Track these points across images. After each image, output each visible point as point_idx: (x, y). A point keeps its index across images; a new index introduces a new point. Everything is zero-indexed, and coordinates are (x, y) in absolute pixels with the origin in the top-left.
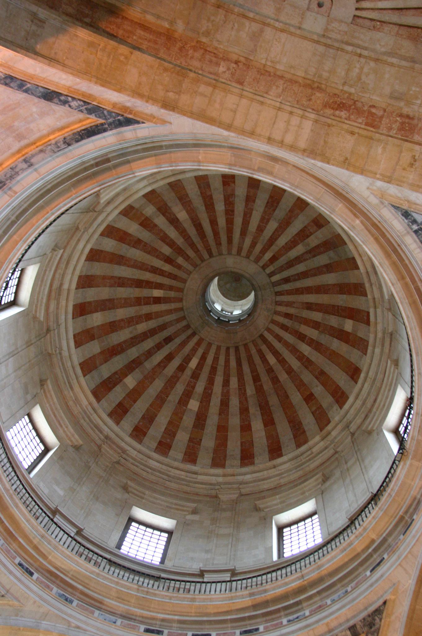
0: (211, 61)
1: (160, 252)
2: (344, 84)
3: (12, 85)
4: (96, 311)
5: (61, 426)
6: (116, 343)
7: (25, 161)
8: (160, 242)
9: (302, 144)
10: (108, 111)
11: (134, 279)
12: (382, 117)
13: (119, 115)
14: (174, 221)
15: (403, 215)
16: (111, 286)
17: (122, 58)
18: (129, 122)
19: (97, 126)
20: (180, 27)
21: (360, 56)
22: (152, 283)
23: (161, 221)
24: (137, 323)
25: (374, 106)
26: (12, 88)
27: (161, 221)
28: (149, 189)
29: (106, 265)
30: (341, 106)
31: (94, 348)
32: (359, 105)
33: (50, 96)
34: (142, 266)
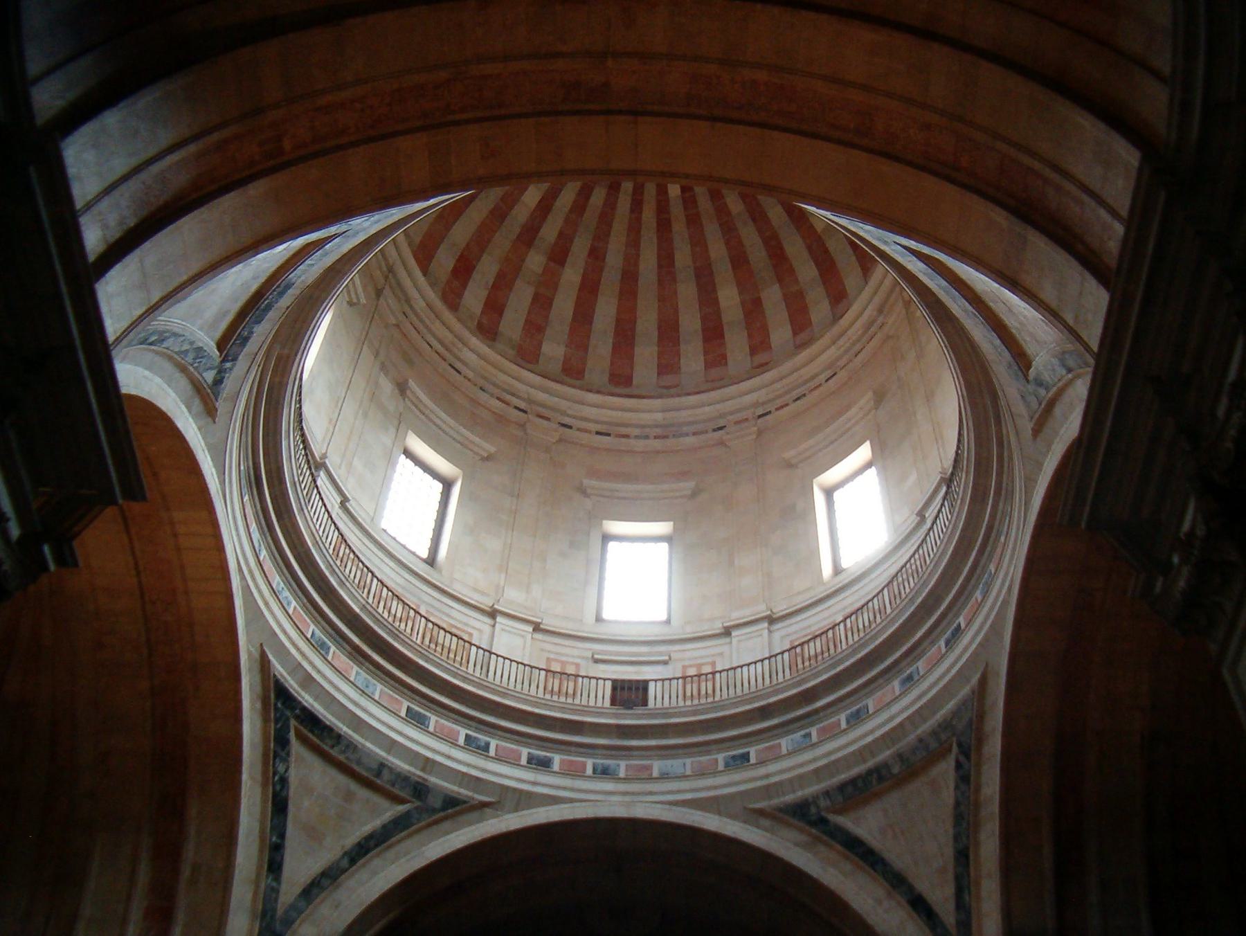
1: (605, 204)
4: (716, 302)
5: (849, 429)
6: (764, 253)
7: (379, 774)
8: (587, 214)
10: (276, 723)
11: (659, 238)
13: (276, 709)
14: (545, 207)
16: (674, 280)
18: (282, 693)
19: (301, 722)
22: (659, 202)
23: (549, 232)
24: (729, 213)
27: (549, 232)
28: (474, 341)
29: (641, 303)
31: (772, 296)
33: (279, 806)
34: (635, 228)
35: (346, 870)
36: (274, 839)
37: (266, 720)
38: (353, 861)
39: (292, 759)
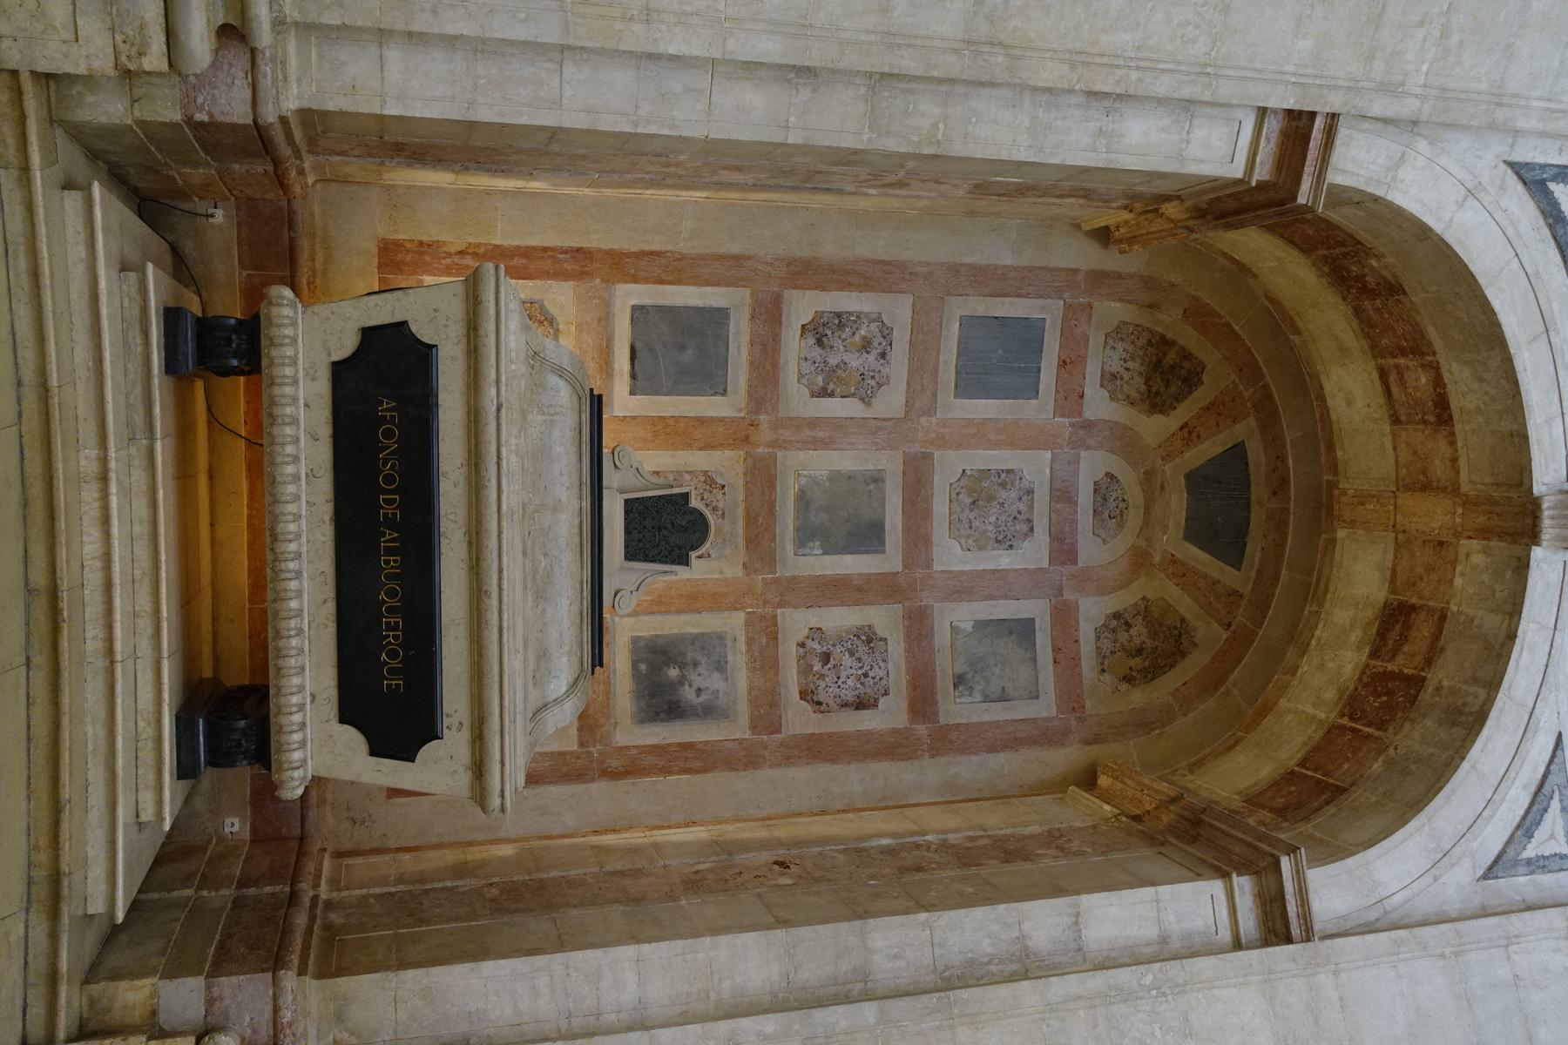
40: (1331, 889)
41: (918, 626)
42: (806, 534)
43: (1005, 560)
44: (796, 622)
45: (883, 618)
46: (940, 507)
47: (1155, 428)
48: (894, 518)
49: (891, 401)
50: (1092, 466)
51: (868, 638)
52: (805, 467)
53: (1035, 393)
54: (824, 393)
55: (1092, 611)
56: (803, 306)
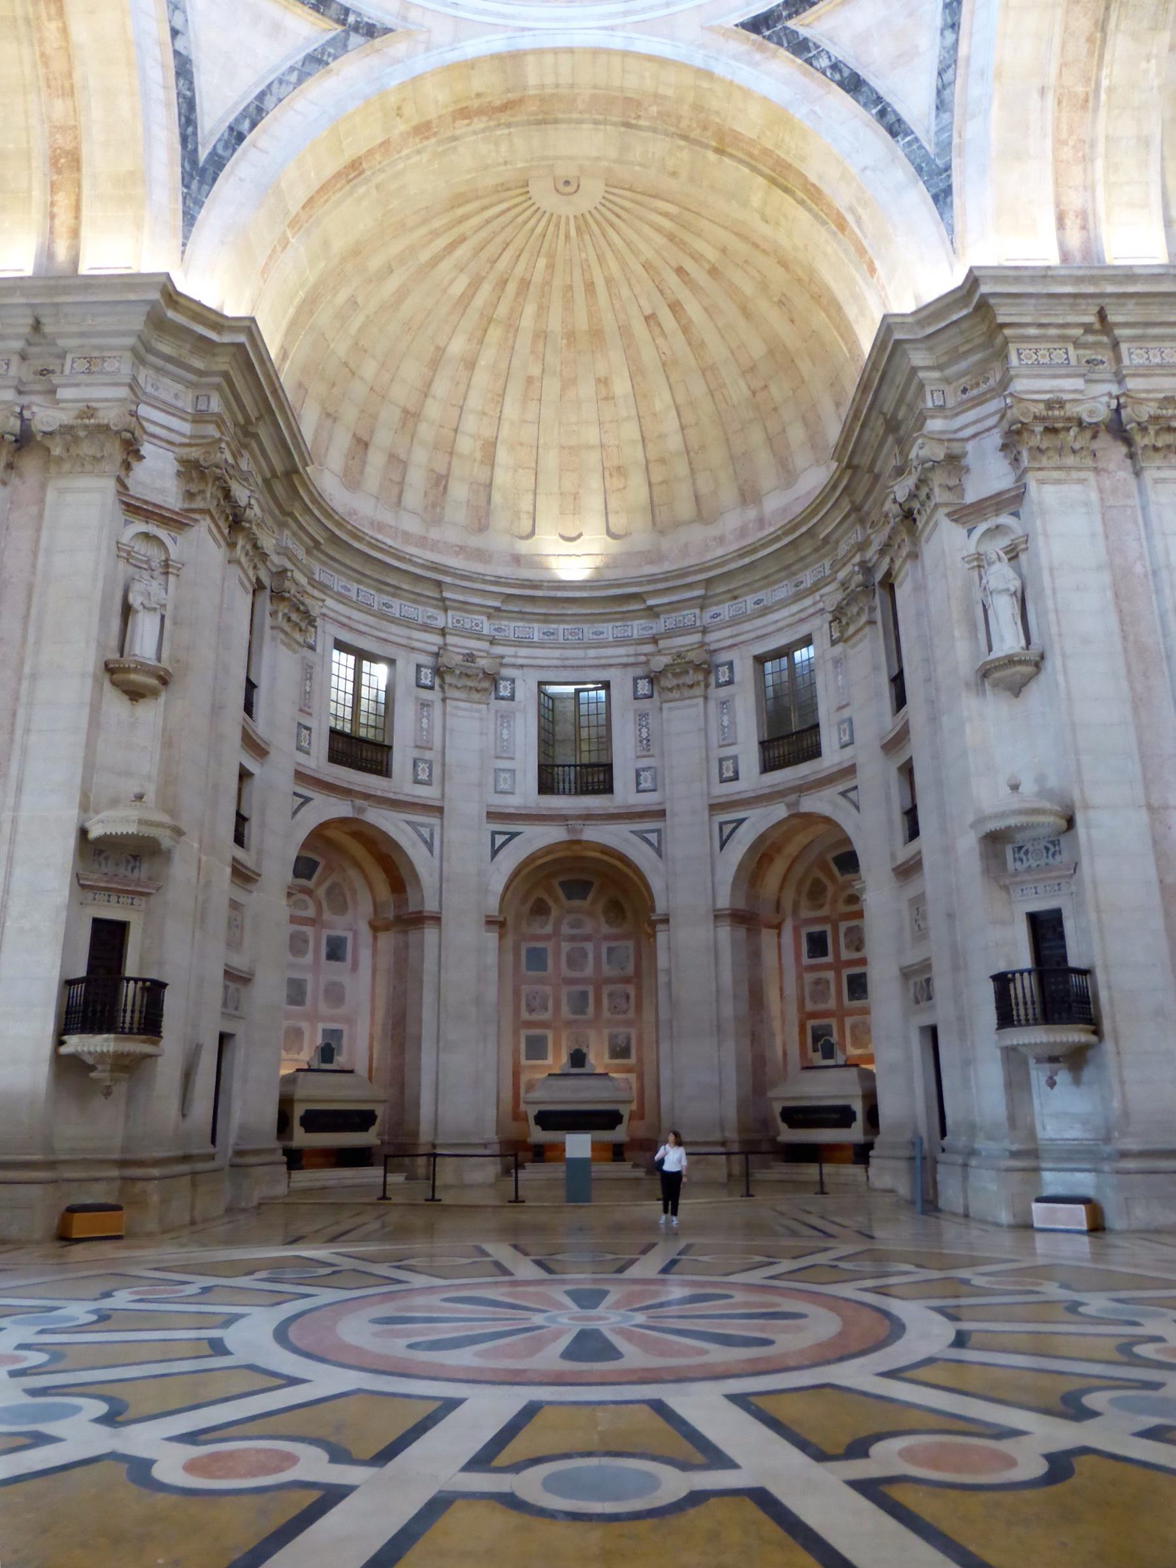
0: (669, 116)
2: (510, 134)
3: (891, 118)
9: (531, 60)
12: (454, 121)
13: (769, 38)
15: (374, 25)
17: (768, 133)
18: (757, 25)
19: (797, 13)
20: (712, 156)
21: (506, 163)
25: (468, 125)
26: (894, 112)
30: (505, 107)
32: (484, 118)
33: (853, 84)
35: (957, 40)
36: (874, 111)
37: (775, 55)
38: (954, 26)
39: (825, 44)
40: (661, 906)
41: (609, 981)
42: (583, 1012)
43: (591, 956)
44: (606, 1014)
45: (606, 990)
46: (576, 974)
47: (555, 912)
48: (579, 988)
49: (548, 989)
50: (565, 930)
51: (610, 995)
52: (566, 1012)
53: (545, 949)
54: (547, 1009)
55: (606, 929)
56: (525, 1015)
